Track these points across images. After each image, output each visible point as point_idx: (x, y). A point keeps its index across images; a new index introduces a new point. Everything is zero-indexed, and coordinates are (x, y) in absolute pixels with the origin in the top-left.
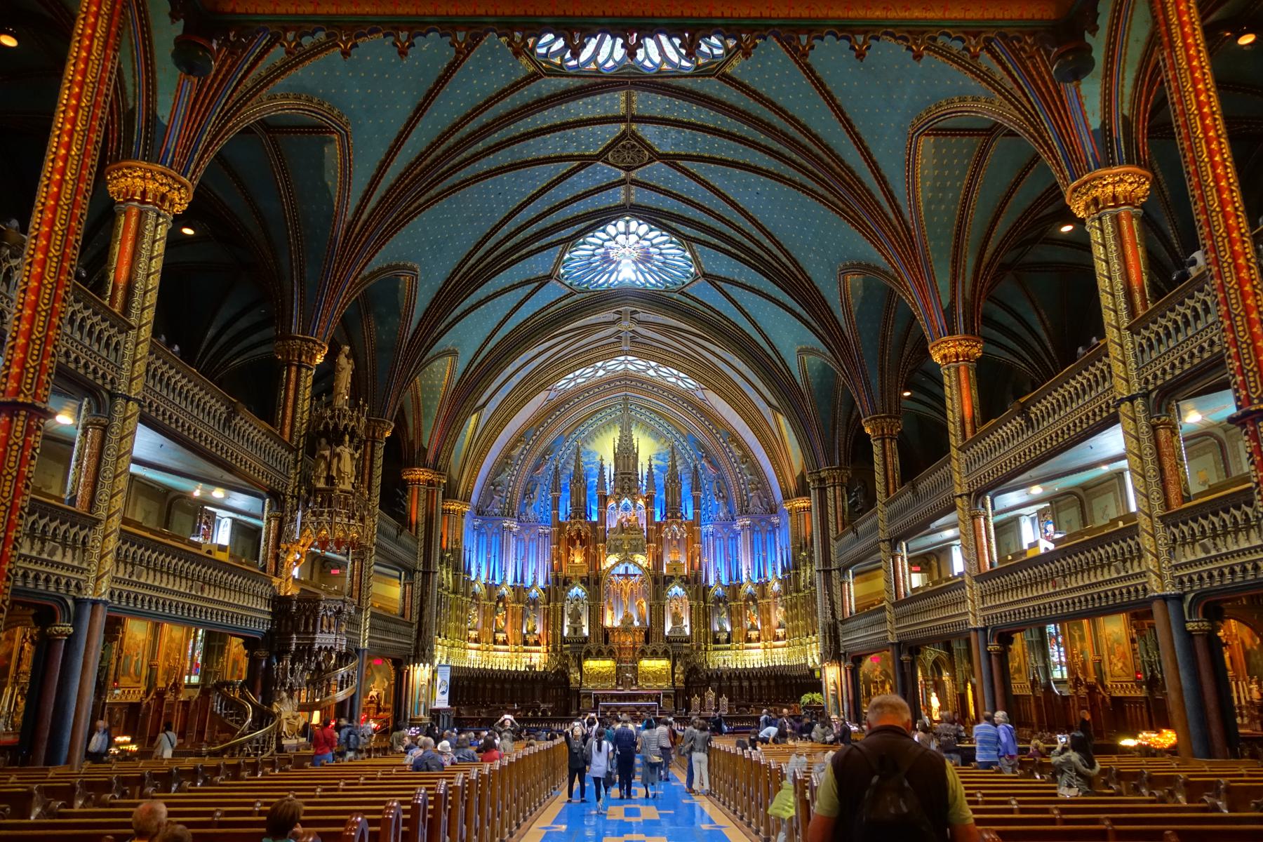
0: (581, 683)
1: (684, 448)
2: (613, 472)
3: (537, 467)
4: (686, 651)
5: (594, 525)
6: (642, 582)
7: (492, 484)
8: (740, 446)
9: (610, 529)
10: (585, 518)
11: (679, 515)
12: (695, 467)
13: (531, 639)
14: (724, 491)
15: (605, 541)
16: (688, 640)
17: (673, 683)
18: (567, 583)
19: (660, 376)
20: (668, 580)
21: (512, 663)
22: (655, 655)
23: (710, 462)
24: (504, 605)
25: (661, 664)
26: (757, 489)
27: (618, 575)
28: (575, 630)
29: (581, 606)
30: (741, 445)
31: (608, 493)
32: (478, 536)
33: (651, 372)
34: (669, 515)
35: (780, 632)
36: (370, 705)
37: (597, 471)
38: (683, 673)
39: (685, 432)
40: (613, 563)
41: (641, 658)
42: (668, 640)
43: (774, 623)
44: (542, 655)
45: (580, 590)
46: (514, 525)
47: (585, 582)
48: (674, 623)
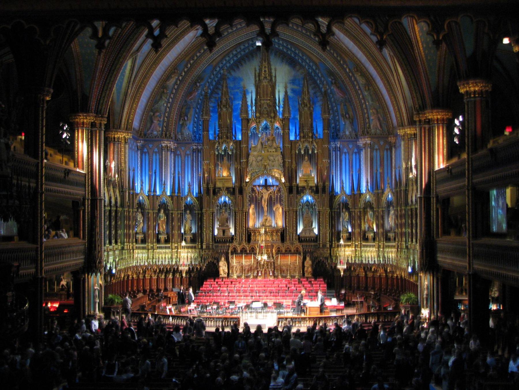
3: (189, 93)
5: (238, 143)
6: (279, 191)
7: (152, 111)
10: (231, 139)
12: (326, 92)
14: (351, 113)
16: (316, 239)
18: (216, 192)
20: (300, 191)
21: (172, 258)
22: (288, 252)
23: (338, 87)
24: (164, 212)
27: (259, 186)
28: (224, 232)
30: (365, 74)
31: (250, 117)
32: (141, 155)
35: (391, 235)
36: (61, 292)
37: (240, 95)
42: (300, 239)
43: (387, 227)
45: (227, 199)
46: (172, 145)
47: (231, 191)
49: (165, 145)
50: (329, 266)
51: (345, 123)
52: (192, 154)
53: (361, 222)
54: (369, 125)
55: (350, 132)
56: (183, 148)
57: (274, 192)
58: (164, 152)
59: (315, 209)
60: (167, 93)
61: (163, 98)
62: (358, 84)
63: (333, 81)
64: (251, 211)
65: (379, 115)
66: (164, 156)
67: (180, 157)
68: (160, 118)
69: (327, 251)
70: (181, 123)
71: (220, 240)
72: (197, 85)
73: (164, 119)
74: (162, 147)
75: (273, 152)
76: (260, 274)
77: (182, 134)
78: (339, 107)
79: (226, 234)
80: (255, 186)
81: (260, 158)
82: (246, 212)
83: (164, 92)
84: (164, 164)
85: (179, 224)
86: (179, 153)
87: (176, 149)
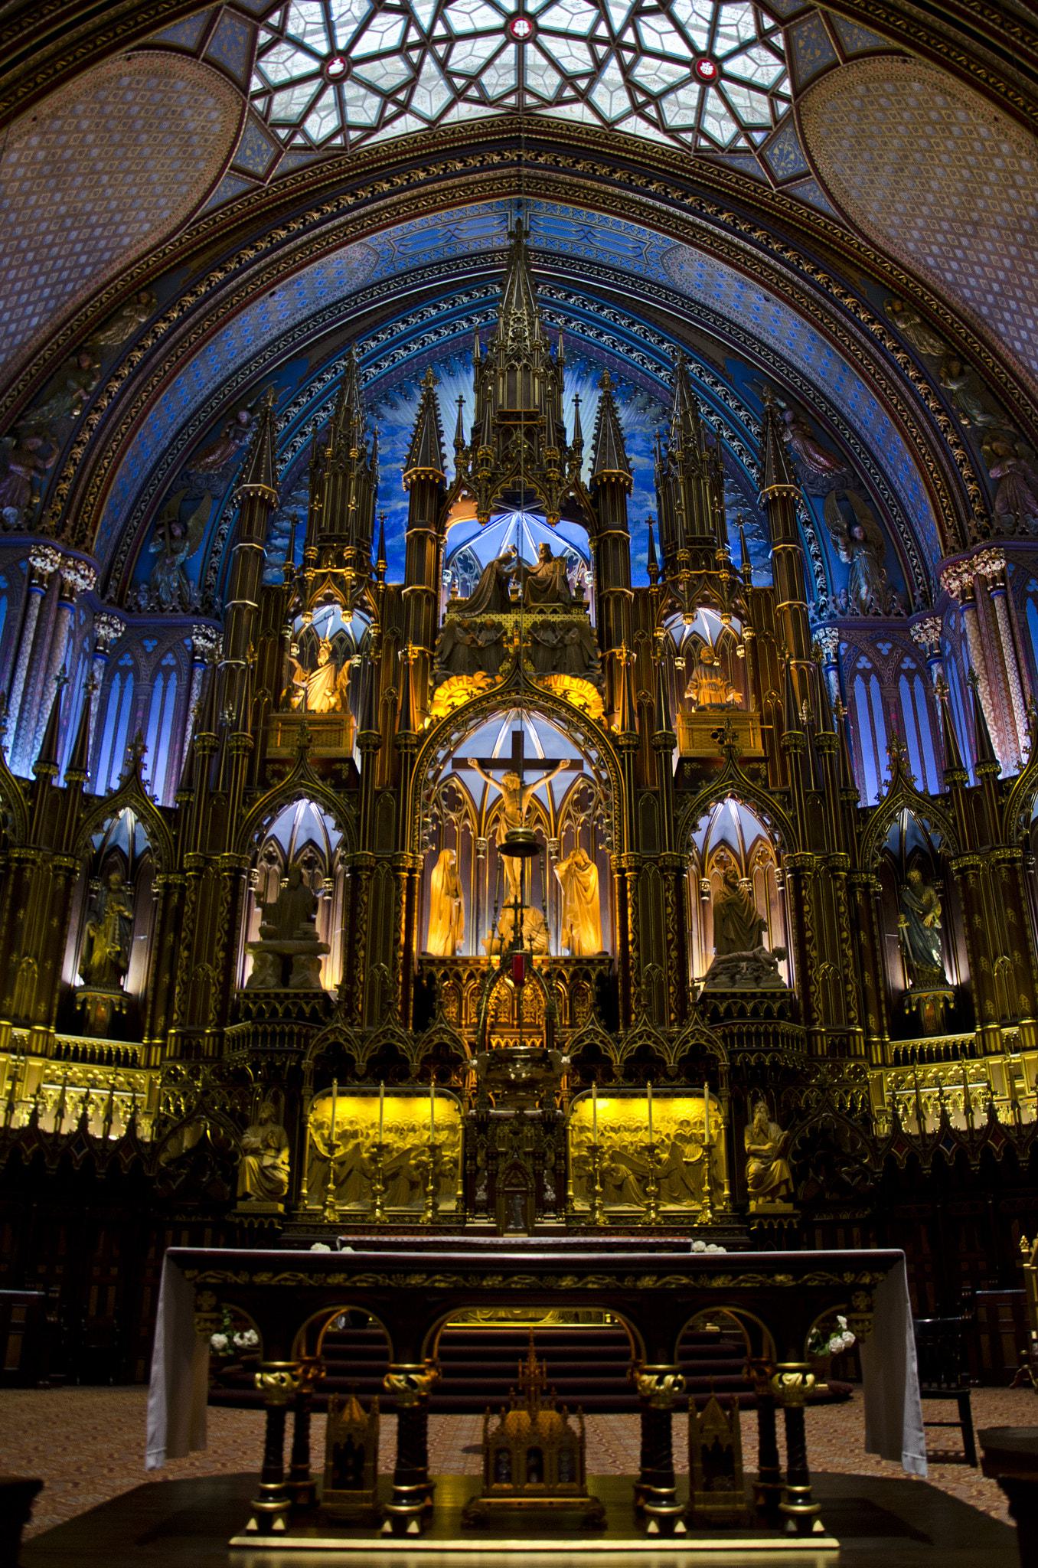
0: (293, 1198)
1: (719, 406)
2: (469, 422)
4: (790, 1057)
6: (582, 801)
7: (13, 433)
8: (932, 325)
9: (451, 605)
11: (719, 556)
13: (100, 1004)
15: (429, 636)
16: (796, 1007)
17: (740, 1197)
19: (644, 101)
23: (809, 437)
25: (688, 1109)
26: (1017, 456)
27: (486, 764)
29: (325, 884)
33: (611, 99)
34: (683, 554)
38: (781, 1154)
39: (718, 355)
40: (460, 702)
41: (579, 1092)
44: (141, 1077)
45: (314, 806)
48: (723, 943)
49: (50, 569)
50: (876, 1159)
51: (851, 556)
52: (185, 669)
53: (1020, 914)
54: (988, 506)
55: (875, 591)
56: (150, 645)
57: (556, 815)
58: (37, 599)
59: (767, 873)
60: (90, 369)
61: (73, 385)
62: (915, 360)
63: (788, 416)
64: (437, 878)
65: (1023, 462)
66: (35, 612)
67: (131, 676)
68: (46, 459)
69: (857, 1073)
70: (152, 550)
71: (261, 1011)
72: (239, 422)
73: (61, 466)
74: (32, 577)
75: (555, 612)
76: (481, 1195)
77: (154, 587)
78: (816, 502)
79: (294, 980)
80: (461, 764)
81: (492, 635)
82: (412, 871)
83: (79, 366)
84: (27, 649)
85: (55, 923)
86: (130, 663)
87: (120, 646)
